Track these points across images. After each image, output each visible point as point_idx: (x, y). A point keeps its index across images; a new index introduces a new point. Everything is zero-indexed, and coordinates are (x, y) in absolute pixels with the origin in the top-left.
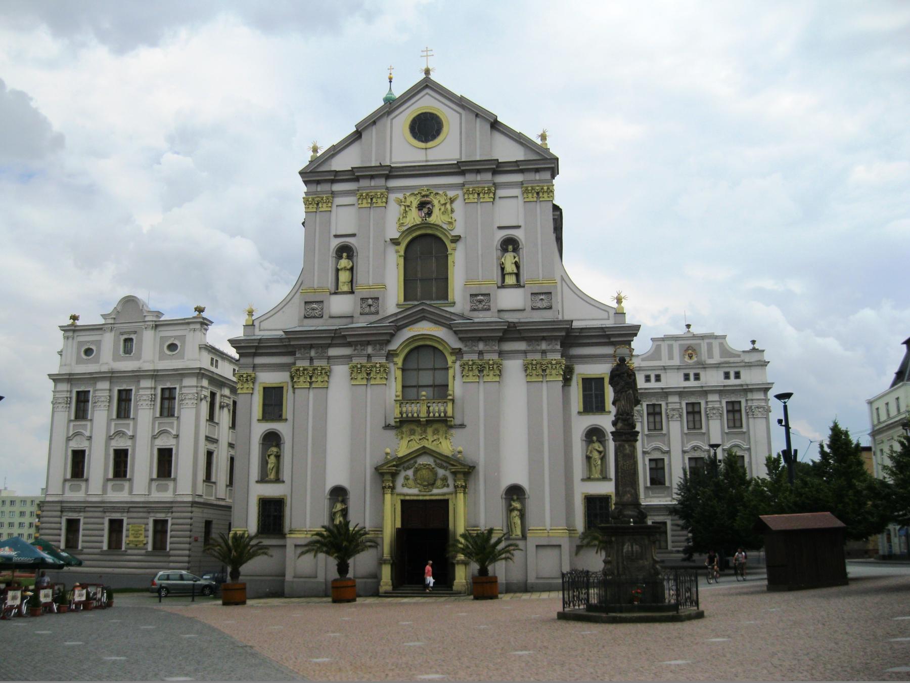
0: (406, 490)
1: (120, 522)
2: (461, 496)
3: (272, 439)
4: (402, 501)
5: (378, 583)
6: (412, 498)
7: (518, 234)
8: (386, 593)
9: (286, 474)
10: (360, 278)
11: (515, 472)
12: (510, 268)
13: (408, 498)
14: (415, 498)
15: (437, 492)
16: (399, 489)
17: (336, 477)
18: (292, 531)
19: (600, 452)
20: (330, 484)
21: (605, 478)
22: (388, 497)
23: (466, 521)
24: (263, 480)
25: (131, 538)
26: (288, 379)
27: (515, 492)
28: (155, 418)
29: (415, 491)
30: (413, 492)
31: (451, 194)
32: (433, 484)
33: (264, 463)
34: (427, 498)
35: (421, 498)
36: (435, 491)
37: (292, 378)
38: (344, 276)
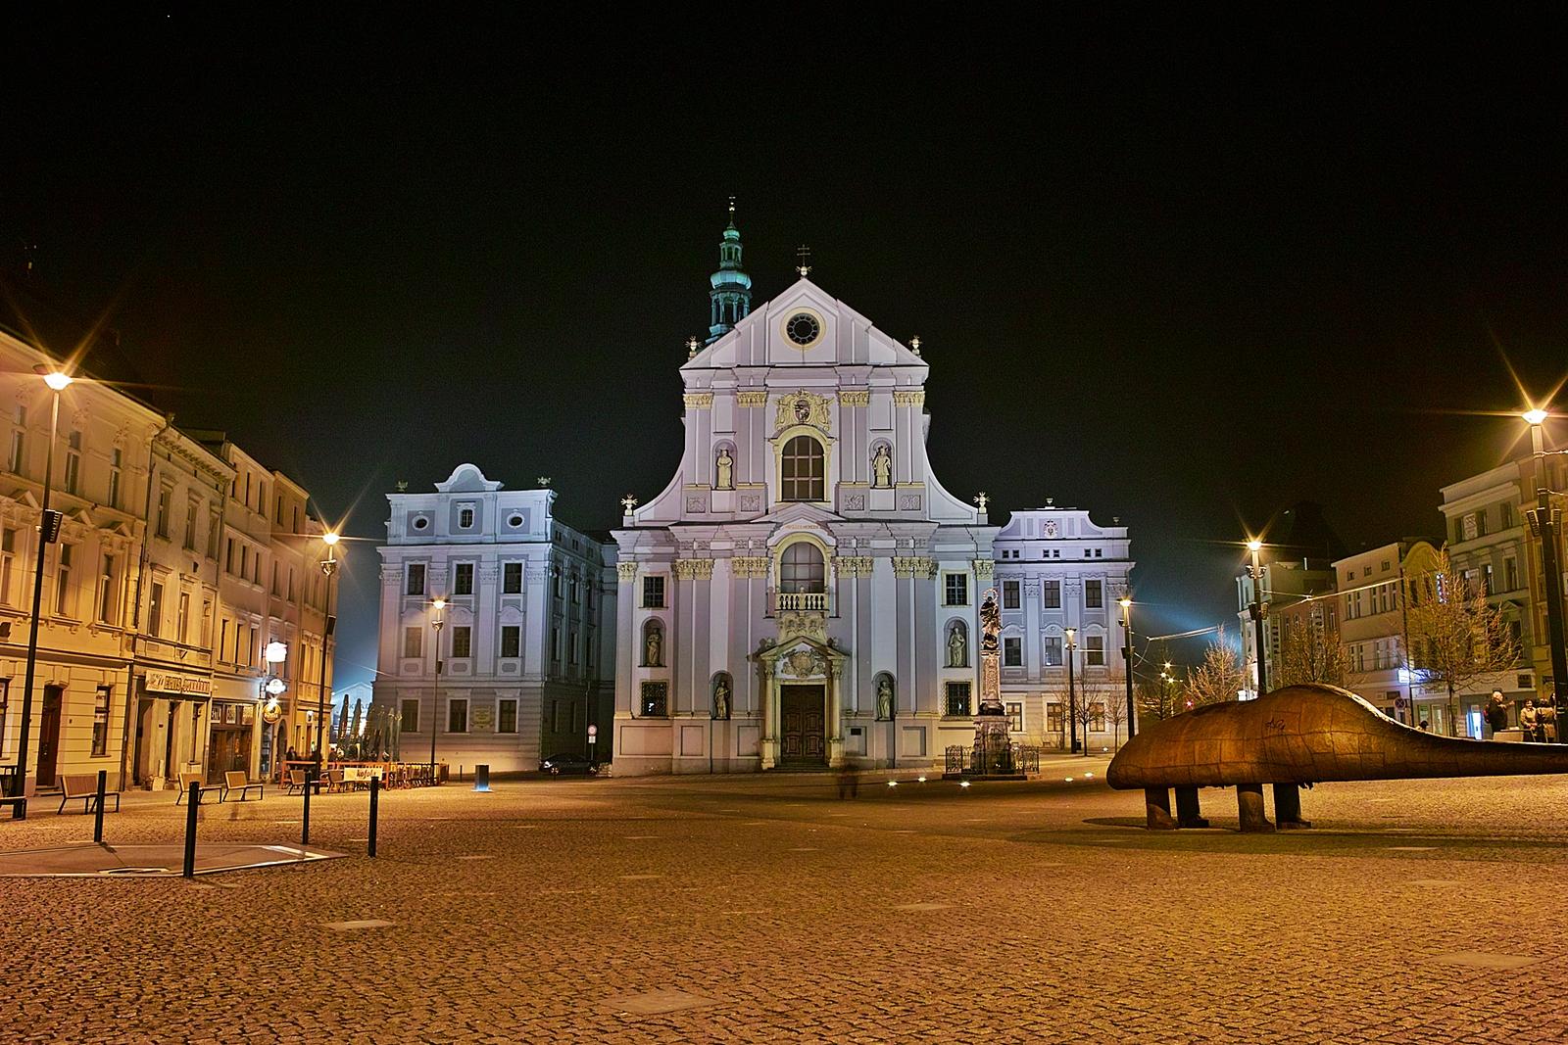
0: (785, 676)
1: (860, 734)
2: (837, 682)
3: (652, 629)
4: (782, 686)
5: (761, 761)
6: (791, 683)
7: (891, 437)
8: (769, 768)
9: (669, 659)
10: (740, 476)
11: (884, 661)
12: (883, 471)
13: (787, 683)
14: (794, 684)
15: (817, 678)
16: (780, 675)
17: (719, 663)
18: (676, 713)
19: (962, 643)
20: (713, 670)
21: (965, 665)
22: (770, 682)
23: (842, 704)
24: (646, 664)
25: (477, 719)
26: (669, 569)
27: (887, 681)
28: (498, 593)
29: (794, 677)
30: (791, 678)
31: (826, 396)
32: (810, 671)
33: (646, 650)
34: (805, 683)
35: (799, 683)
36: (812, 677)
37: (673, 568)
38: (725, 473)
